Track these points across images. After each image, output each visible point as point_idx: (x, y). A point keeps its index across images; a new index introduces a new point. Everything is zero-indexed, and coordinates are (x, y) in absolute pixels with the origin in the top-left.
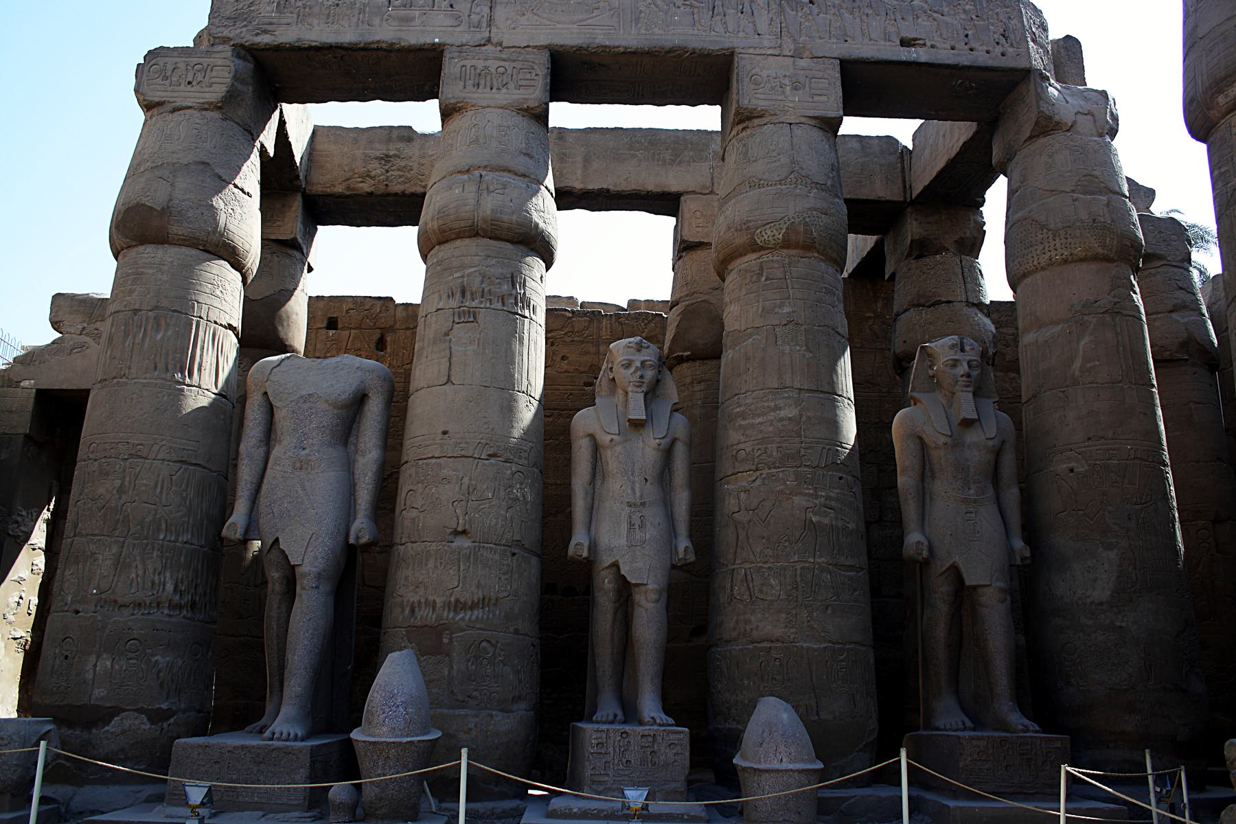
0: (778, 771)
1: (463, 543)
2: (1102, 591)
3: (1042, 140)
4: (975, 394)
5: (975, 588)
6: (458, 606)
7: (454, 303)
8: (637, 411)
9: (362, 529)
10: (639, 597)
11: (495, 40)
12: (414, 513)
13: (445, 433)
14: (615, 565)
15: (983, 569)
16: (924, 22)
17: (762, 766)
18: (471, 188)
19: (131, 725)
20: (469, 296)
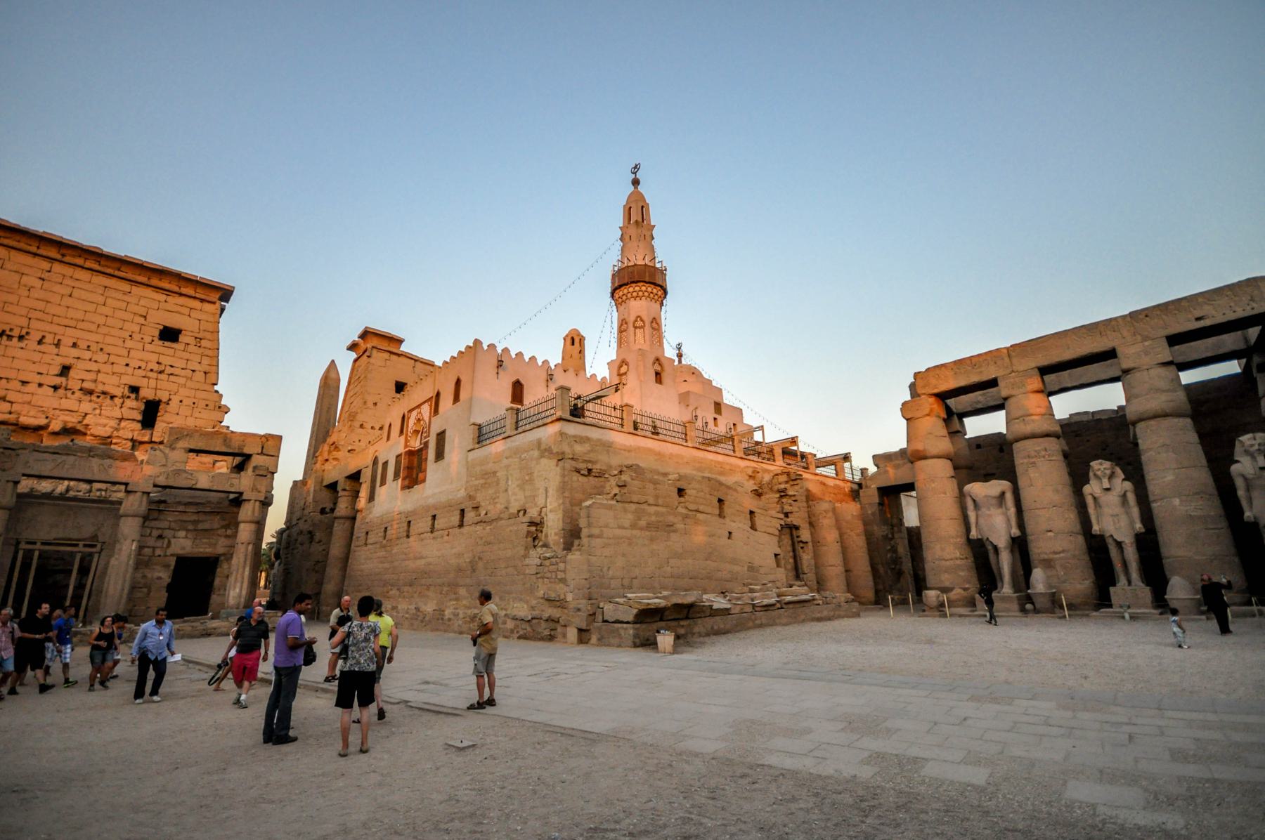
6: (1055, 553)
9: (1015, 532)
16: (1206, 307)
19: (957, 593)
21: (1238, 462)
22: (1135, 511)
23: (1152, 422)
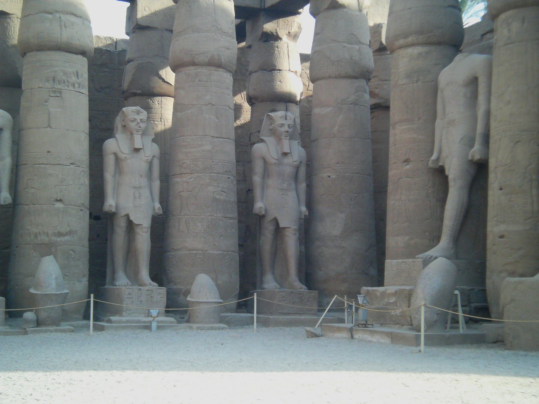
0: (207, 302)
1: (59, 205)
2: (337, 231)
3: (333, 12)
4: (290, 139)
5: (284, 228)
6: (60, 234)
7: (48, 85)
10: (138, 230)
12: (33, 191)
13: (49, 152)
14: (127, 216)
15: (289, 220)
17: (200, 301)
21: (262, 141)
22: (157, 184)
23: (204, 70)
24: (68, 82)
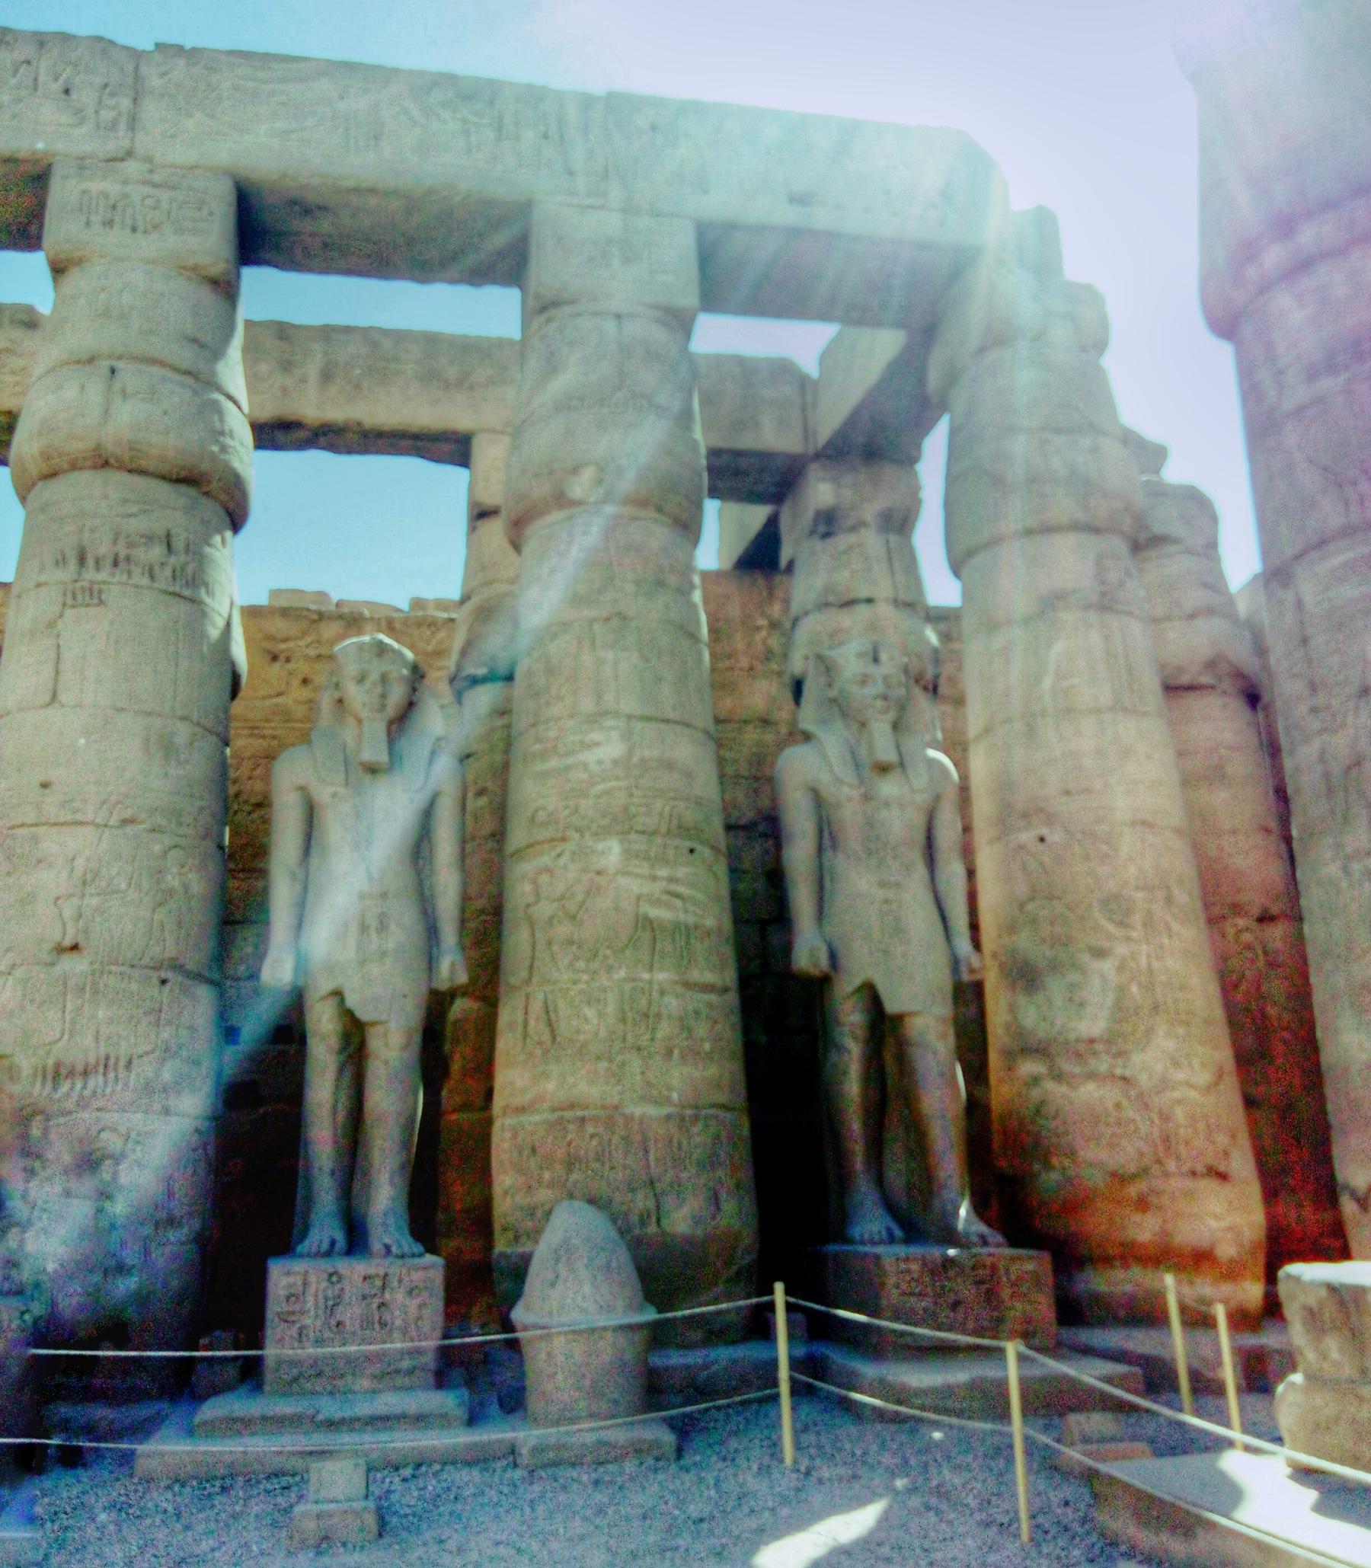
1: (76, 966)
8: (374, 751)
10: (375, 1043)
11: (140, 150)
13: (45, 785)
14: (338, 994)
18: (95, 392)
20: (90, 562)
24: (128, 559)
